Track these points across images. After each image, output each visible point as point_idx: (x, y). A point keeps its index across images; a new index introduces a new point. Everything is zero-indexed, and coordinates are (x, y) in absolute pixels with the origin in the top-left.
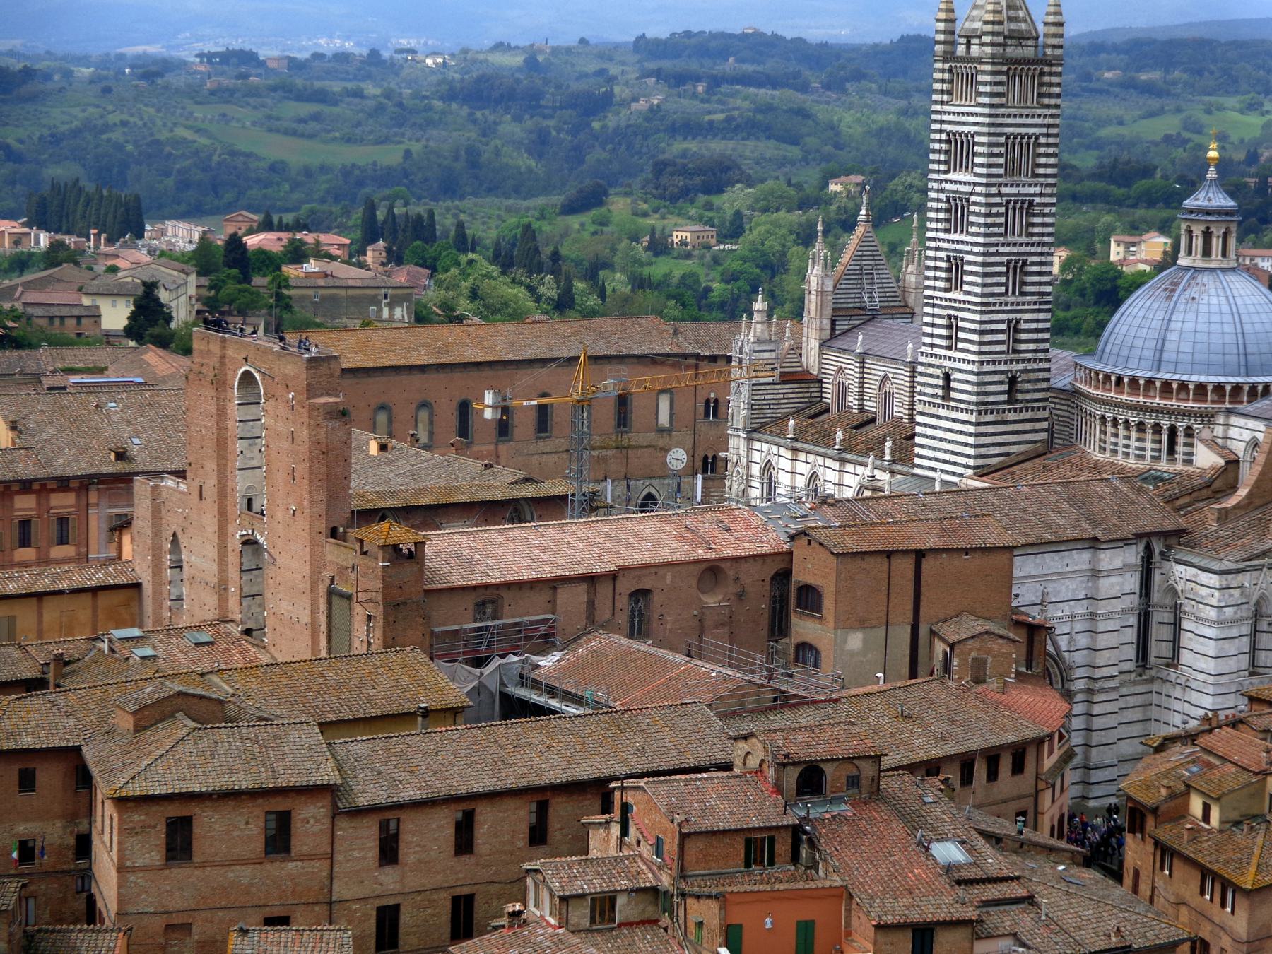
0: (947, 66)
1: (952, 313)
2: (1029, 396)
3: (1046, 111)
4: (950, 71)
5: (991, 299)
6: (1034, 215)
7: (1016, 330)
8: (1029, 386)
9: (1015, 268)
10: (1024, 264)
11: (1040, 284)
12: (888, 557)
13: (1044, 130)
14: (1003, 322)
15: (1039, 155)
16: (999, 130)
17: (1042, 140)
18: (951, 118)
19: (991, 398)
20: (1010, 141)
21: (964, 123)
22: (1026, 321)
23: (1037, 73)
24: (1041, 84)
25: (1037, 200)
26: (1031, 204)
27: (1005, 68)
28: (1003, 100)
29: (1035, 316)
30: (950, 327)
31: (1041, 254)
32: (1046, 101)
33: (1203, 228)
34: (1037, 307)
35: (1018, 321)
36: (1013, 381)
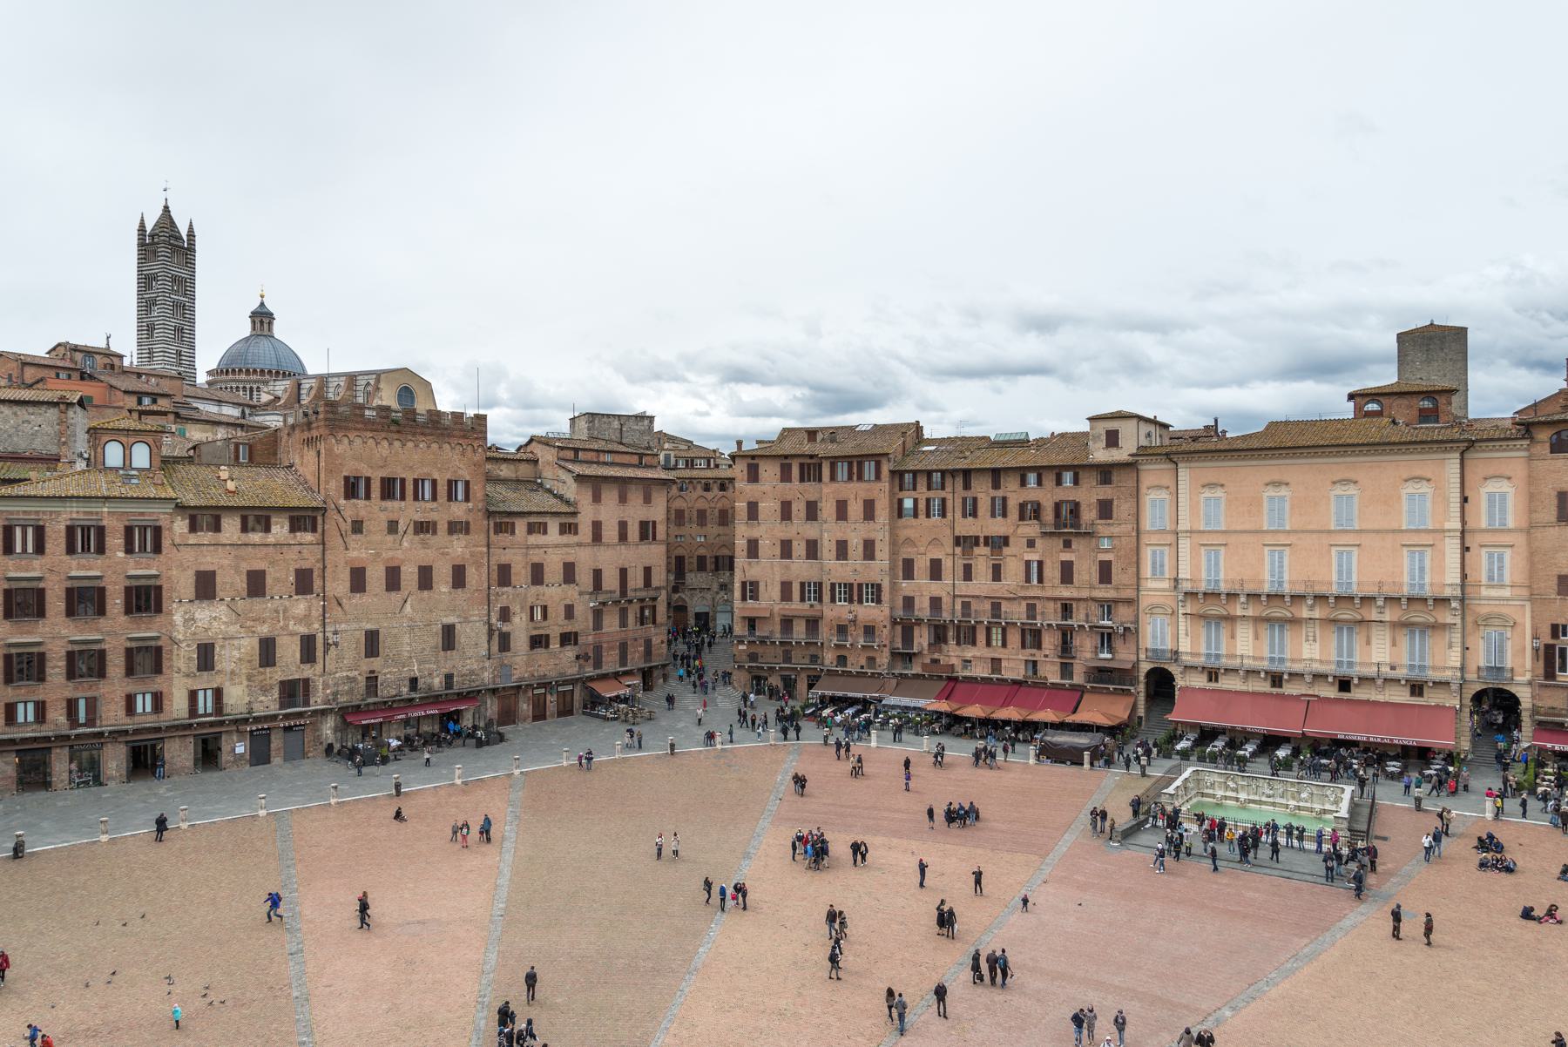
26: (184, 305)
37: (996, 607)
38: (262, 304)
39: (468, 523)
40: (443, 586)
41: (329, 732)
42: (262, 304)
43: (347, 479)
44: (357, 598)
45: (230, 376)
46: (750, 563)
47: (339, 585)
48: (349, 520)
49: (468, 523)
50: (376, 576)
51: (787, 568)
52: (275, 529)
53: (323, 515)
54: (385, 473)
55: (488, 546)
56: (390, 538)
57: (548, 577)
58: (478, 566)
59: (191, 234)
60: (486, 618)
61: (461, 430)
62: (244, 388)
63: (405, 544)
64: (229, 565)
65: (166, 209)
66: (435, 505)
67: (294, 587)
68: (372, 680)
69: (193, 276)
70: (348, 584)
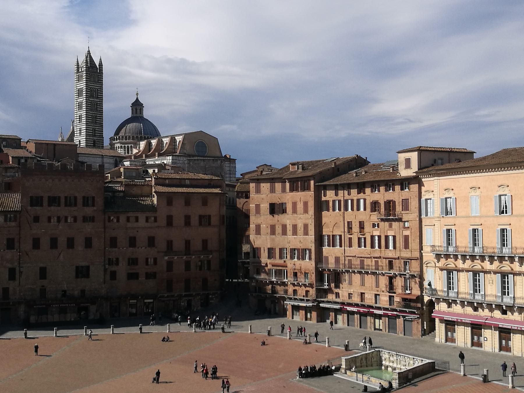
1: (80, 127)
4: (78, 76)
5: (88, 123)
7: (95, 131)
10: (96, 116)
13: (99, 88)
14: (91, 128)
16: (88, 86)
17: (99, 90)
18: (79, 85)
19: (89, 144)
24: (98, 78)
25: (98, 103)
26: (97, 104)
27: (89, 73)
30: (80, 131)
32: (99, 81)
35: (95, 129)
36: (94, 141)
37: (362, 262)
38: (137, 99)
39: (93, 217)
40: (80, 247)
41: (22, 312)
42: (137, 99)
43: (31, 197)
46: (257, 238)
47: (27, 245)
48: (33, 216)
49: (93, 217)
50: (45, 242)
51: (273, 240)
55: (105, 228)
59: (101, 64)
60: (103, 263)
62: (125, 147)
63: (60, 227)
65: (89, 51)
66: (75, 208)
68: (43, 291)
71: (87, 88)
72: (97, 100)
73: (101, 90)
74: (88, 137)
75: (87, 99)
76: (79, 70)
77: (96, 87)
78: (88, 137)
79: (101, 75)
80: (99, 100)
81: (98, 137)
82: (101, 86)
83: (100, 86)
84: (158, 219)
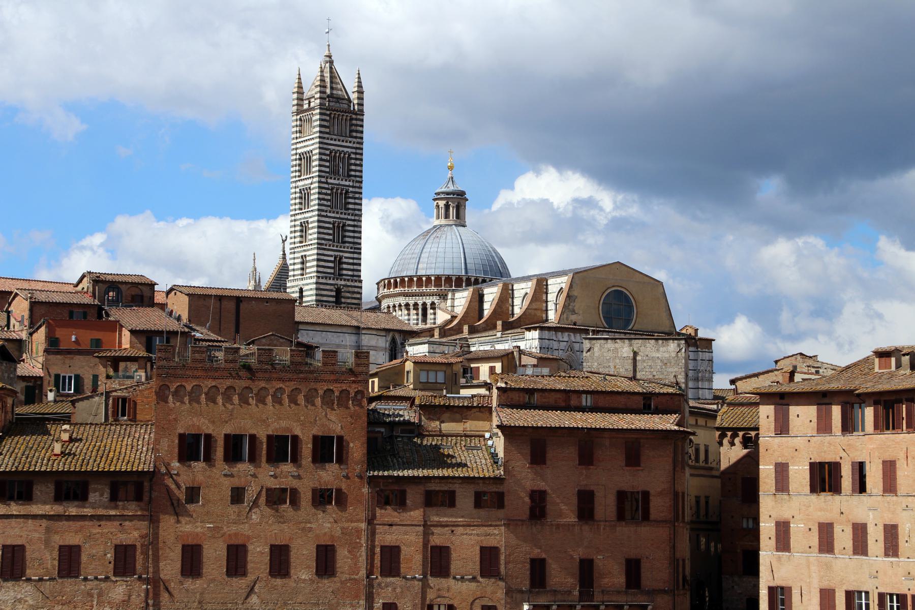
0: (298, 117)
1: (303, 254)
2: (349, 301)
3: (354, 140)
4: (301, 120)
5: (323, 242)
6: (350, 198)
7: (341, 263)
8: (348, 295)
9: (338, 227)
10: (344, 225)
11: (354, 237)
12: (220, 300)
13: (354, 151)
14: (331, 256)
15: (352, 164)
16: (325, 146)
17: (353, 156)
18: (302, 145)
19: (325, 299)
20: (333, 154)
21: (307, 146)
22: (346, 258)
23: (349, 118)
24: (351, 125)
25: (351, 189)
26: (347, 192)
27: (328, 112)
28: (327, 130)
29: (351, 255)
30: (303, 263)
31: (354, 220)
32: (354, 134)
33: (444, 202)
34: (352, 250)
35: (341, 258)
36: (338, 291)
43: (182, 437)
44: (189, 583)
45: (433, 289)
46: (779, 558)
51: (828, 567)
52: (93, 497)
53: (151, 480)
54: (228, 429)
56: (235, 508)
57: (456, 566)
58: (354, 548)
61: (332, 373)
62: (416, 305)
64: (40, 539)
67: (112, 566)
69: (359, 151)
70: (178, 565)
71: (323, 151)
72: (347, 183)
73: (358, 156)
74: (324, 281)
75: (323, 180)
76: (302, 106)
77: (346, 150)
78: (324, 281)
79: (358, 117)
80: (351, 184)
81: (348, 280)
82: (358, 146)
83: (355, 145)
84: (815, 541)
